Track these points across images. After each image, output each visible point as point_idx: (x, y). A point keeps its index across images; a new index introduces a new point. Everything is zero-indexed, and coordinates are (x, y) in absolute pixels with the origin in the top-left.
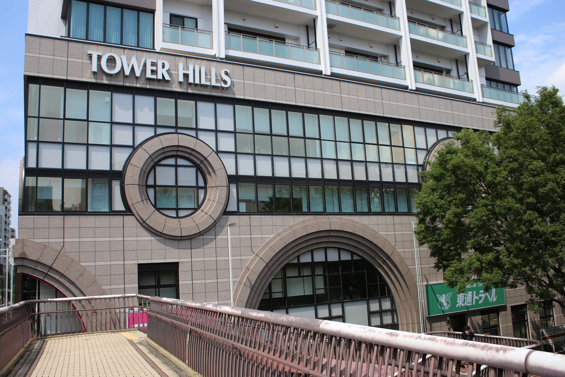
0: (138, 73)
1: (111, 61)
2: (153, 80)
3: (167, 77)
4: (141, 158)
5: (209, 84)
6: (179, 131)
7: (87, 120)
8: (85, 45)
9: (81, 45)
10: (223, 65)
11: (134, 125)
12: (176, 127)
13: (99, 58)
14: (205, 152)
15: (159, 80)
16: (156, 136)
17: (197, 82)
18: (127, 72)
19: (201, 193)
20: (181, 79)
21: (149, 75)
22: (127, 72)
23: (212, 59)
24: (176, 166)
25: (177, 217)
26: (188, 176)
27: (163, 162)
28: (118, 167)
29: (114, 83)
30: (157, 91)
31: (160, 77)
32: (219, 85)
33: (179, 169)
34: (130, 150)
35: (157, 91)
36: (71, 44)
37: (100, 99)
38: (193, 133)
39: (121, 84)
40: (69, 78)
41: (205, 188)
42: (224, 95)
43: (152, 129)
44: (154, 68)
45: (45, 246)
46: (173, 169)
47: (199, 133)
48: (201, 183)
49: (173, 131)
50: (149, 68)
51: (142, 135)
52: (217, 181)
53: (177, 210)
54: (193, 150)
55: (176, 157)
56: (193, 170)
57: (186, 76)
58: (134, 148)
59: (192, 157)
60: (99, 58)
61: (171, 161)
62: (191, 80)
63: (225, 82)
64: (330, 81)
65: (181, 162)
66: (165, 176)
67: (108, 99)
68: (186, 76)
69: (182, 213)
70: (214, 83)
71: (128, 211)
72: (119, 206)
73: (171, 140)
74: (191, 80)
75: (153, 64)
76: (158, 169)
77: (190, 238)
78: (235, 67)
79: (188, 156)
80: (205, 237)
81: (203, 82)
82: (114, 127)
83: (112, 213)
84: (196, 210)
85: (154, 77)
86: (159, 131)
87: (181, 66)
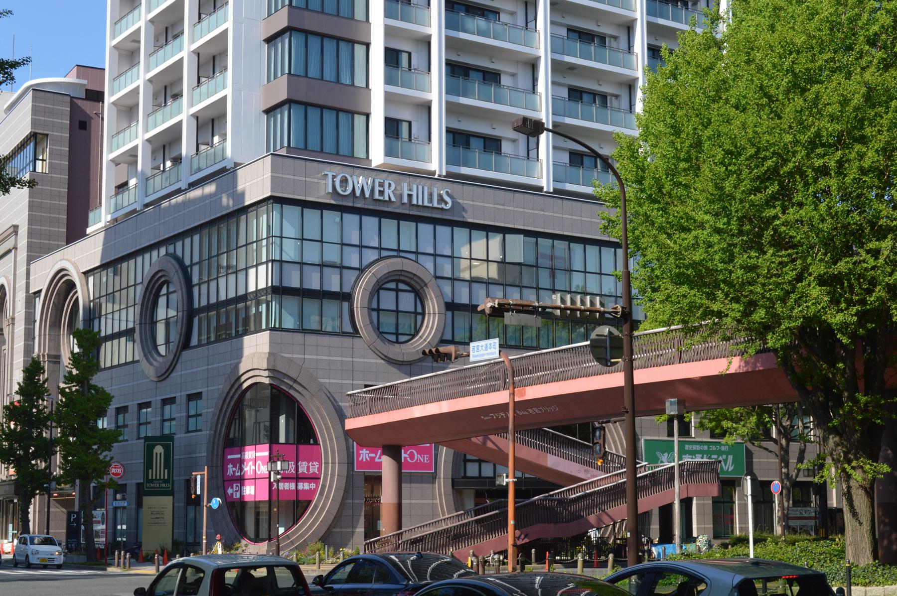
0: (367, 194)
1: (344, 181)
2: (379, 200)
3: (393, 199)
4: (367, 281)
5: (430, 205)
6: (402, 254)
7: (321, 241)
8: (321, 165)
9: (316, 164)
10: (445, 183)
11: (361, 247)
12: (399, 250)
13: (334, 177)
14: (427, 278)
15: (385, 201)
16: (381, 259)
17: (420, 203)
18: (358, 193)
19: (419, 318)
20: (405, 200)
21: (377, 196)
22: (358, 193)
23: (428, 176)
24: (397, 290)
25: (397, 342)
26: (407, 302)
27: (385, 286)
28: (347, 290)
29: (345, 204)
30: (380, 212)
31: (387, 198)
32: (440, 206)
33: (400, 294)
34: (357, 272)
35: (380, 212)
36: (308, 163)
37: (332, 218)
38: (413, 257)
39: (350, 204)
40: (308, 199)
41: (423, 314)
42: (445, 217)
43: (376, 252)
44: (381, 189)
45: (290, 360)
46: (394, 293)
47: (420, 256)
48: (419, 310)
49: (395, 253)
50: (377, 189)
51: (371, 256)
52: (433, 305)
53: (397, 334)
54: (415, 275)
55: (397, 281)
56: (412, 295)
57: (410, 196)
58: (361, 270)
59: (413, 283)
60: (334, 177)
61: (392, 285)
62: (414, 202)
63: (446, 203)
64: (551, 200)
65: (402, 286)
66: (387, 300)
67: (338, 220)
68: (410, 196)
69: (402, 338)
70: (436, 205)
71: (355, 333)
72: (348, 328)
73: (395, 264)
74: (414, 202)
75: (381, 185)
76: (382, 292)
77: (410, 363)
78: (456, 186)
79: (409, 280)
80: (423, 364)
81: (426, 204)
82: (344, 247)
83: (344, 334)
84: (414, 336)
85: (381, 198)
86: (385, 253)
87: (405, 186)
